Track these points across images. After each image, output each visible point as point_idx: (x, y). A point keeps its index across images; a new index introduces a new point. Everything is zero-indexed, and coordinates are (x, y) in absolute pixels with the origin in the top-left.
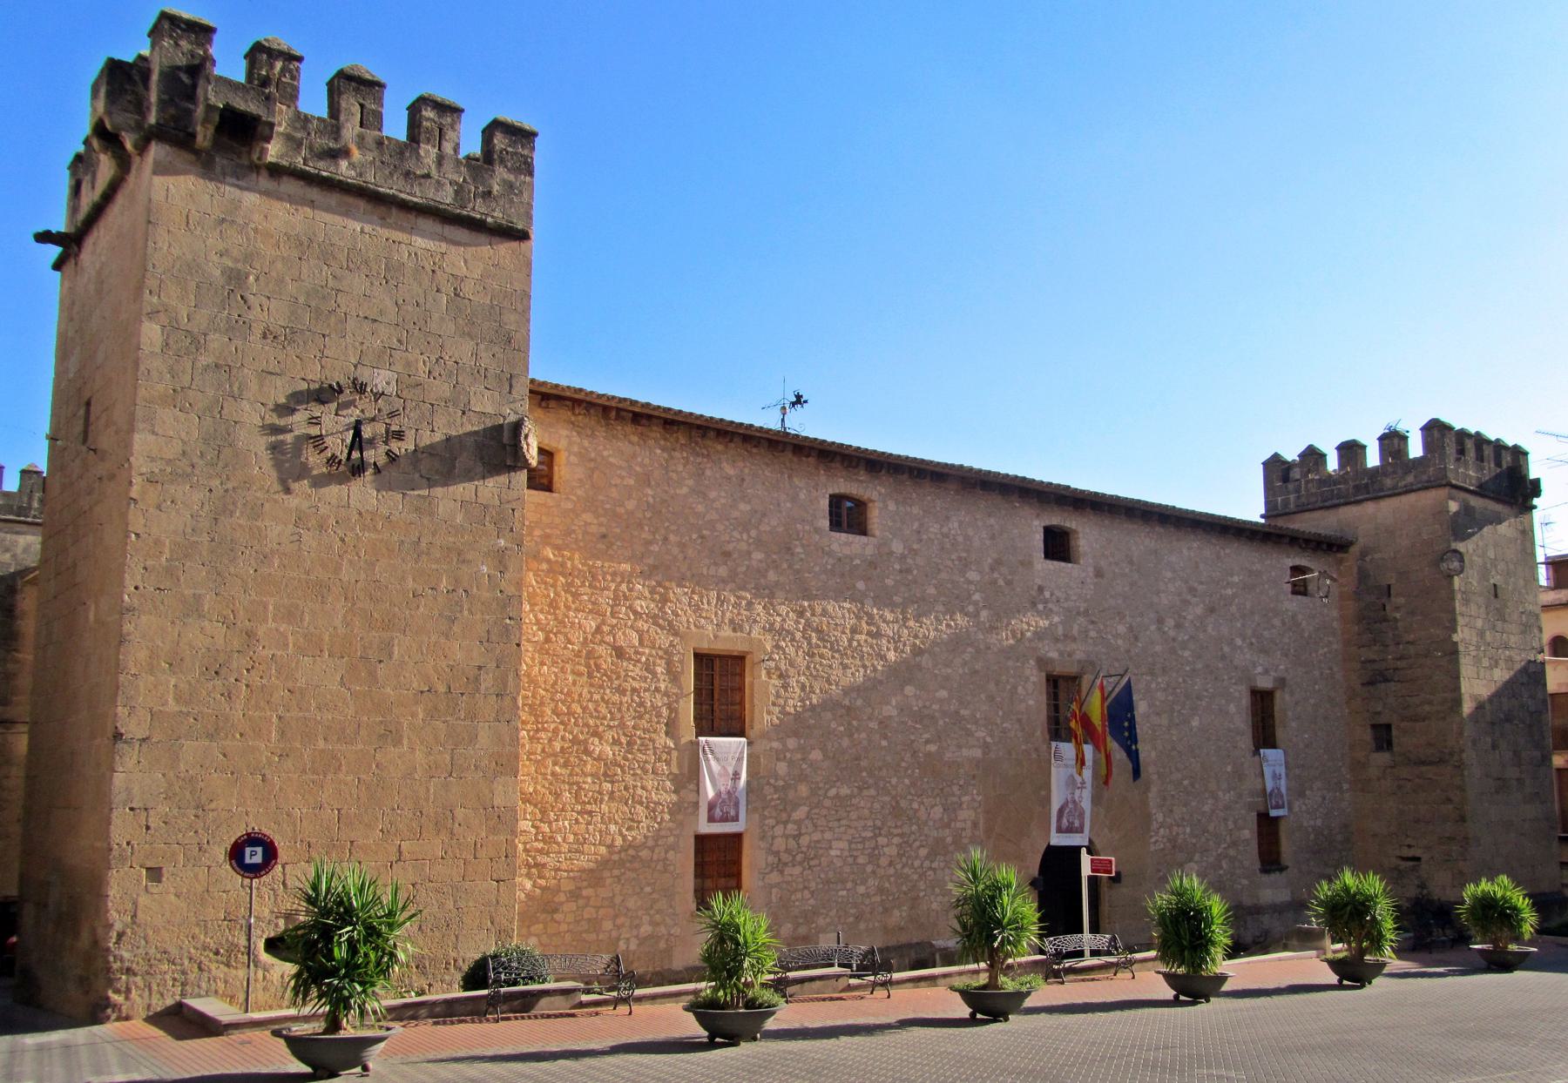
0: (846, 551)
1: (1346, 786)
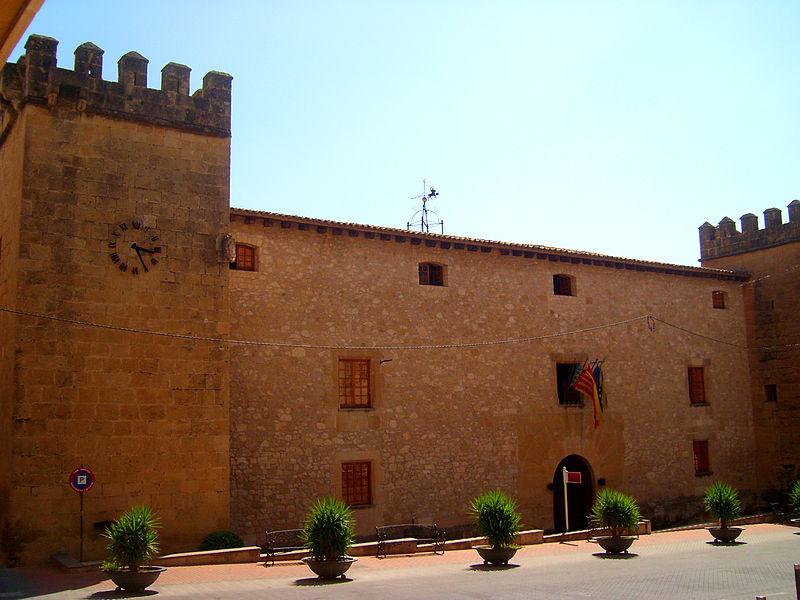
0: (430, 295)
1: (750, 423)
